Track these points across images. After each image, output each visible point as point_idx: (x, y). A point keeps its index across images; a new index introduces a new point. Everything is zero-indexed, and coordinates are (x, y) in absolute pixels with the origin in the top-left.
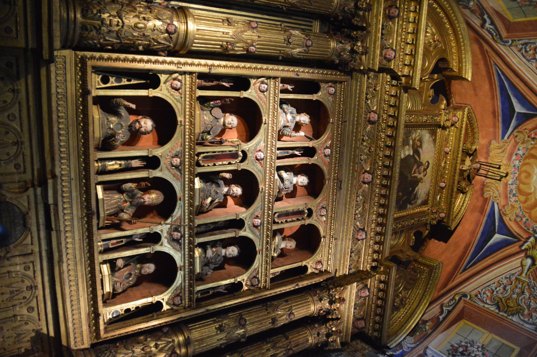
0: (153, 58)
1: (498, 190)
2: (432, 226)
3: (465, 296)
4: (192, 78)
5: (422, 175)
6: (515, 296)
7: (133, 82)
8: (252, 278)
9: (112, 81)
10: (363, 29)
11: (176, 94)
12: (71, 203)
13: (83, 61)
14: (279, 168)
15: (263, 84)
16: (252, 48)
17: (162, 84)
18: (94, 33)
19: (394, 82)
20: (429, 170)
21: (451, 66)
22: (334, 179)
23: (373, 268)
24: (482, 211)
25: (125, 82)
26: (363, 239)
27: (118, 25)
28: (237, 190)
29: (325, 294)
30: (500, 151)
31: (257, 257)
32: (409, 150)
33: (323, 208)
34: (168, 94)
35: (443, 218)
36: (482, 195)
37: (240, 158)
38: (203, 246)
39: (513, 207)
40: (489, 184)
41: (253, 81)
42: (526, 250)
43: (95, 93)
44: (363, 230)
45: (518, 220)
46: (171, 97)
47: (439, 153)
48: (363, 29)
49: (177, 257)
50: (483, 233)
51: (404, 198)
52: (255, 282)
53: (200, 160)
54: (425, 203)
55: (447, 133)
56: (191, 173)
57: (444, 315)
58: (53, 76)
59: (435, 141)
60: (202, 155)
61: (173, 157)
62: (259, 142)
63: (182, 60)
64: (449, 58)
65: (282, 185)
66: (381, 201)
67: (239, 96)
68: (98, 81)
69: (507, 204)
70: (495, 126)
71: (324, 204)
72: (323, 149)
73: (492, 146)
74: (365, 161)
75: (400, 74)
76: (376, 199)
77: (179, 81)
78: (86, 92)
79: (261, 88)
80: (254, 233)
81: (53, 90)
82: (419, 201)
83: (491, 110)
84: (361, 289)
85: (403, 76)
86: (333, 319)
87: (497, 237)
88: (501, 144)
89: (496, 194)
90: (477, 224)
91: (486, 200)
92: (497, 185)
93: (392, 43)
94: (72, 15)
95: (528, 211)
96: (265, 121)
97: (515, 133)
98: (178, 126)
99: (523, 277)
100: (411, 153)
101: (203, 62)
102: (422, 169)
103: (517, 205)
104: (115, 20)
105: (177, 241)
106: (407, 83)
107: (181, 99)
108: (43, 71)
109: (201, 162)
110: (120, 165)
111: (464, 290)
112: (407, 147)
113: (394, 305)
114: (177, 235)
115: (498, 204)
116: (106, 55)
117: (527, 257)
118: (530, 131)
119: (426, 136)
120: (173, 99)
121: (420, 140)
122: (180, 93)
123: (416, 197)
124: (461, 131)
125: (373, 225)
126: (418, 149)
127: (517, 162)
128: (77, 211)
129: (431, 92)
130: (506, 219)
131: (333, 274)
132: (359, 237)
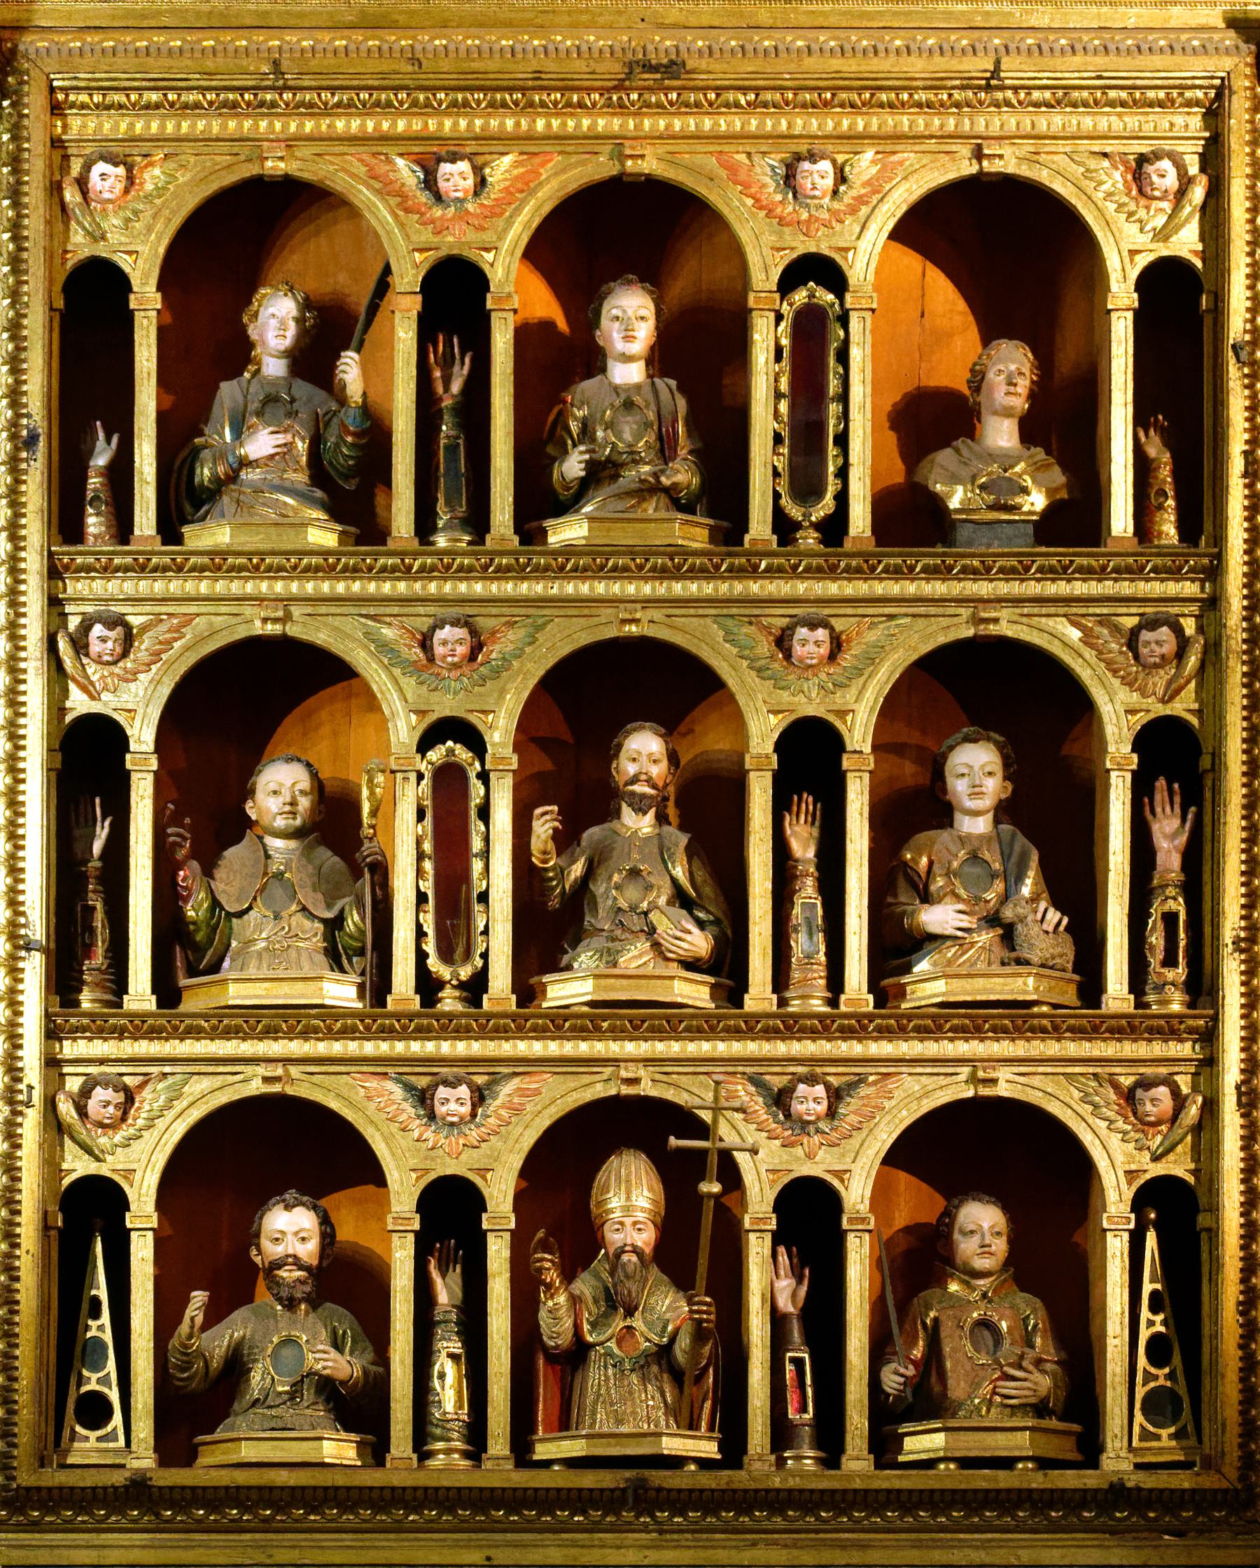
4: (77, 1029)
7: (101, 1291)
8: (1137, 657)
9: (99, 1381)
11: (148, 1100)
15: (87, 646)
17: (104, 1170)
25: (101, 1328)
34: (150, 1137)
37: (463, 754)
41: (79, 703)
43: (143, 1459)
46: (161, 1124)
52: (1160, 641)
53: (455, 975)
60: (433, 963)
61: (432, 1116)
62: (384, 647)
67: (150, 777)
68: (99, 1439)
71: (766, 170)
72: (438, 212)
77: (86, 1092)
79: (107, 658)
80: (871, 659)
96: (276, 620)
98: (289, 1091)
107: (170, 1080)
120: (170, 1115)
122: (142, 1086)
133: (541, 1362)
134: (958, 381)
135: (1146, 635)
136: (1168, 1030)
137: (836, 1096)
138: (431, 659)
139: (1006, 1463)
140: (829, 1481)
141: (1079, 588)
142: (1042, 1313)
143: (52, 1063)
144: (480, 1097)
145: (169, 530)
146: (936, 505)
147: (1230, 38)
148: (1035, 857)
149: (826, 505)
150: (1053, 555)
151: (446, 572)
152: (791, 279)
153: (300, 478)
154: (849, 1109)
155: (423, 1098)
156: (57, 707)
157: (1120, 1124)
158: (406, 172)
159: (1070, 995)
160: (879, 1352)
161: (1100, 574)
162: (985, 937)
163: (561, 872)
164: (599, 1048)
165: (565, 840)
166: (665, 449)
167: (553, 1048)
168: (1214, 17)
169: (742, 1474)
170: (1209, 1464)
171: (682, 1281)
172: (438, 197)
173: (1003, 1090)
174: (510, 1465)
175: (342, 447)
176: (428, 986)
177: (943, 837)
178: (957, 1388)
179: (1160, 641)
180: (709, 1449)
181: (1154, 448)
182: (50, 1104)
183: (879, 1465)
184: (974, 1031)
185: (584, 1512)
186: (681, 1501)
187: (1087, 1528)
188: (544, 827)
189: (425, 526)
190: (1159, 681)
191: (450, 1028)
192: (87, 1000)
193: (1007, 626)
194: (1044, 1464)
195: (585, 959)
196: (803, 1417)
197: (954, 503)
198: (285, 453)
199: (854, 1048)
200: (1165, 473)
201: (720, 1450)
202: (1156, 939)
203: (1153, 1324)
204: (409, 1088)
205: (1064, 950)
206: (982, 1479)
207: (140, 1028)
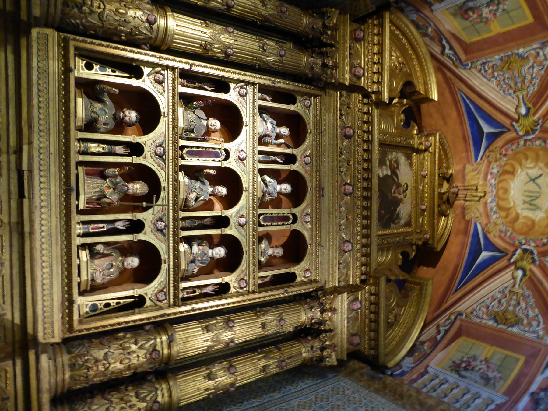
2: (418, 247)
3: (460, 314)
4: (174, 74)
5: (402, 196)
6: (511, 308)
10: (332, 46)
11: (159, 87)
13: (66, 41)
14: (262, 172)
16: (229, 50)
18: (76, 10)
19: (366, 101)
20: (408, 192)
21: (418, 89)
22: (316, 187)
23: (363, 282)
24: (466, 232)
26: (349, 251)
27: (99, 7)
28: (222, 190)
29: (316, 304)
30: (475, 173)
31: (244, 257)
32: (386, 169)
33: (307, 214)
34: (152, 87)
35: (428, 240)
37: (224, 157)
38: (189, 240)
39: (495, 224)
40: (469, 207)
41: (232, 86)
42: (515, 262)
44: (349, 241)
45: (503, 235)
46: (155, 89)
47: (417, 176)
48: (332, 46)
49: (161, 247)
50: (470, 253)
51: (387, 216)
52: (243, 284)
54: (408, 224)
55: (421, 157)
56: (175, 164)
57: (441, 335)
59: (411, 164)
60: (186, 150)
61: (157, 147)
62: (240, 145)
63: (165, 56)
64: (415, 81)
65: (265, 189)
66: (364, 213)
69: (489, 222)
70: (467, 151)
71: (309, 211)
73: (467, 170)
74: (345, 174)
75: (370, 90)
76: (359, 211)
78: (67, 70)
82: (402, 222)
85: (374, 92)
86: (326, 331)
87: (485, 255)
88: (475, 166)
89: (477, 214)
90: (463, 246)
91: (468, 223)
93: (360, 63)
95: (511, 225)
97: (487, 154)
98: (162, 117)
99: (517, 289)
100: (389, 173)
102: (402, 190)
103: (499, 221)
105: (161, 231)
106: (377, 98)
109: (185, 155)
110: (103, 148)
111: (458, 309)
112: (384, 167)
113: (388, 323)
114: (161, 225)
115: (480, 223)
117: (517, 268)
118: (501, 148)
119: (402, 160)
120: (157, 92)
121: (397, 162)
122: (163, 87)
123: (398, 217)
124: (435, 154)
125: (358, 238)
126: (396, 170)
127: (493, 181)
128: (55, 188)
129: (402, 116)
130: (491, 236)
131: (322, 284)
132: (347, 249)
133: (102, 169)
135: (244, 282)
136: (176, 296)
138: (239, 152)
139: (79, 275)
142: (114, 278)
148: (205, 265)
150: (257, 263)
152: (294, 216)
154: (159, 234)
155: (160, 145)
157: (157, 289)
160: (106, 244)
161: (253, 272)
162: (192, 257)
163: (201, 176)
169: (75, 214)
170: (80, 322)
171: (121, 200)
172: (305, 157)
174: (77, 160)
176: (182, 148)
178: (97, 262)
179: (243, 284)
180: (81, 207)
183: (78, 246)
185: (64, 177)
186: (68, 201)
187: (63, 296)
189: (261, 153)
190: (236, 285)
191: (174, 151)
193: (245, 257)
194: (79, 284)
195: (187, 180)
196: (91, 228)
201: (81, 210)
203: (113, 303)
204: (162, 143)
206: (75, 271)
207: (174, 88)
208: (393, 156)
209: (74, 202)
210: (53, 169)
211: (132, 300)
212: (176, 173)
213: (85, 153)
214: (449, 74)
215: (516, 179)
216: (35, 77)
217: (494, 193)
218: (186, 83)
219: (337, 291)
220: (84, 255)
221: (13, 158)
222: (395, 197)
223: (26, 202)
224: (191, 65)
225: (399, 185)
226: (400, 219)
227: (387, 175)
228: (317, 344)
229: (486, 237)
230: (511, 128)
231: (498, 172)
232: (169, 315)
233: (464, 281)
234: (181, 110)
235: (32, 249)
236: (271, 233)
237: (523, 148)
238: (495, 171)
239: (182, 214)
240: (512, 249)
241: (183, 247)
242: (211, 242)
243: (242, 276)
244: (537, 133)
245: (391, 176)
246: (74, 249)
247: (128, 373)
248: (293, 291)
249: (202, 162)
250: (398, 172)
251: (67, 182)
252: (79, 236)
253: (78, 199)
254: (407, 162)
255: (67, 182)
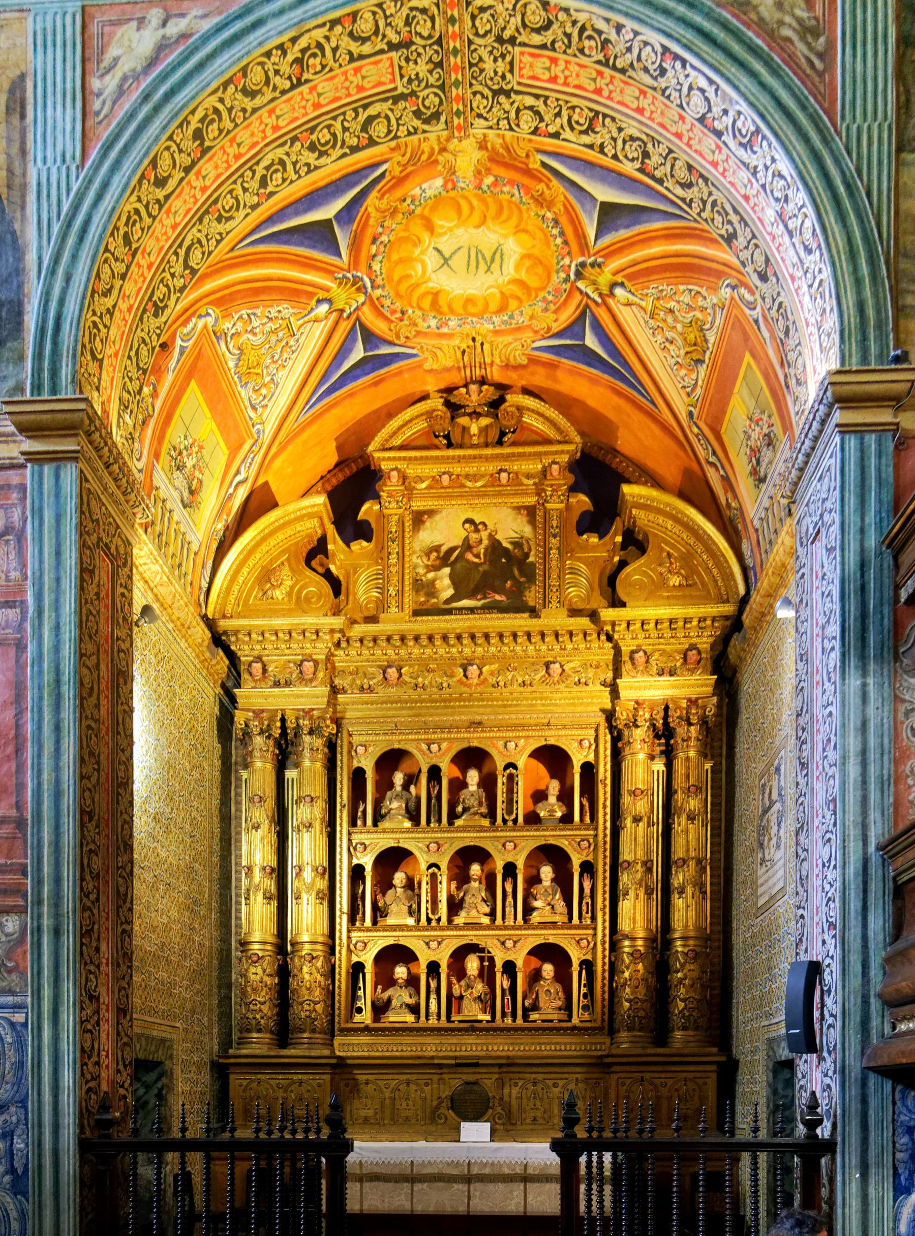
0: (337, 970)
1: (510, 344)
5: (484, 535)
11: (369, 946)
12: (461, 1045)
23: (609, 638)
24: (552, 366)
26: (562, 666)
30: (439, 353)
32: (441, 579)
33: (505, 746)
36: (524, 367)
37: (436, 870)
40: (503, 358)
41: (355, 861)
44: (547, 665)
51: (516, 572)
56: (448, 929)
58: (355, 1054)
60: (430, 916)
70: (399, 373)
71: (501, 744)
73: (435, 367)
78: (366, 1030)
81: (366, 1054)
83: (372, 389)
84: (633, 664)
88: (427, 354)
91: (533, 361)
92: (500, 346)
94: (306, 1041)
100: (447, 570)
101: (338, 920)
104: (306, 1007)
108: (350, 1062)
114: (509, 944)
116: (337, 1012)
123: (517, 544)
132: (560, 671)
134: (543, 787)
136: (587, 927)
137: (515, 942)
139: (551, 1021)
140: (514, 1025)
141: (568, 833)
143: (349, 938)
144: (439, 943)
145: (375, 824)
146: (538, 815)
147: (600, 714)
149: (514, 816)
151: (433, 832)
152: (507, 767)
153: (403, 812)
154: (518, 945)
156: (350, 861)
158: (424, 747)
159: (566, 920)
162: (548, 908)
164: (465, 933)
165: (458, 888)
166: (480, 804)
167: (455, 933)
168: (597, 709)
173: (551, 941)
175: (412, 805)
176: (429, 920)
177: (539, 886)
178: (541, 1004)
179: (585, 844)
180: (488, 1018)
181: (585, 802)
182: (348, 946)
184: (545, 928)
186: (481, 1030)
188: (454, 885)
189: (428, 822)
190: (585, 852)
191: (434, 929)
192: (358, 924)
193: (552, 841)
195: (463, 914)
196: (509, 1011)
197: (542, 814)
198: (400, 807)
199: (520, 932)
200: (587, 808)
202: (584, 908)
203: (584, 990)
205: (565, 910)
207: (368, 930)
208: (419, 561)
209: (484, 1024)
210: (455, 1041)
211: (584, 972)
212: (457, 928)
213: (439, 1015)
214: (274, 450)
215: (447, 288)
216: (377, 1054)
217: (474, 320)
218: (360, 915)
219: (615, 693)
220: (534, 1016)
221: (445, 1070)
222: (485, 554)
223: (481, 1062)
224: (342, 912)
225: (467, 546)
226: (522, 538)
227: (451, 576)
228: (681, 731)
229: (559, 335)
230: (354, 317)
231: (434, 317)
232: (604, 936)
233: (639, 387)
234: (390, 921)
235: (521, 1058)
236: (530, 792)
237: (387, 288)
238: (433, 323)
239: (499, 921)
240: (578, 297)
241: (535, 918)
242: (534, 880)
243: (575, 845)
244: (359, 274)
245: (452, 565)
246: (527, 1025)
247: (652, 981)
248: (604, 771)
249: (443, 897)
250: (444, 549)
251: (466, 1030)
252: (514, 1021)
253: (481, 1021)
254: (428, 524)
255: (466, 1030)
